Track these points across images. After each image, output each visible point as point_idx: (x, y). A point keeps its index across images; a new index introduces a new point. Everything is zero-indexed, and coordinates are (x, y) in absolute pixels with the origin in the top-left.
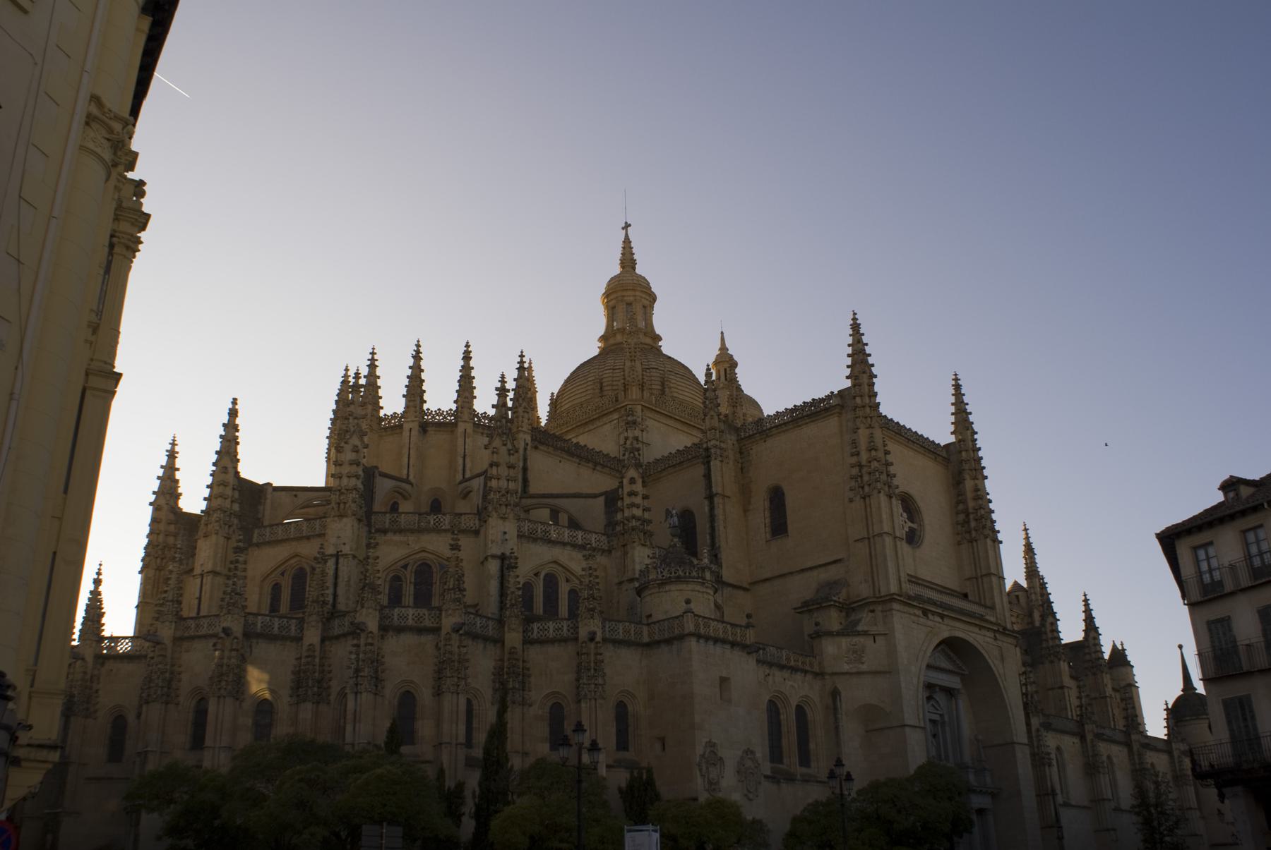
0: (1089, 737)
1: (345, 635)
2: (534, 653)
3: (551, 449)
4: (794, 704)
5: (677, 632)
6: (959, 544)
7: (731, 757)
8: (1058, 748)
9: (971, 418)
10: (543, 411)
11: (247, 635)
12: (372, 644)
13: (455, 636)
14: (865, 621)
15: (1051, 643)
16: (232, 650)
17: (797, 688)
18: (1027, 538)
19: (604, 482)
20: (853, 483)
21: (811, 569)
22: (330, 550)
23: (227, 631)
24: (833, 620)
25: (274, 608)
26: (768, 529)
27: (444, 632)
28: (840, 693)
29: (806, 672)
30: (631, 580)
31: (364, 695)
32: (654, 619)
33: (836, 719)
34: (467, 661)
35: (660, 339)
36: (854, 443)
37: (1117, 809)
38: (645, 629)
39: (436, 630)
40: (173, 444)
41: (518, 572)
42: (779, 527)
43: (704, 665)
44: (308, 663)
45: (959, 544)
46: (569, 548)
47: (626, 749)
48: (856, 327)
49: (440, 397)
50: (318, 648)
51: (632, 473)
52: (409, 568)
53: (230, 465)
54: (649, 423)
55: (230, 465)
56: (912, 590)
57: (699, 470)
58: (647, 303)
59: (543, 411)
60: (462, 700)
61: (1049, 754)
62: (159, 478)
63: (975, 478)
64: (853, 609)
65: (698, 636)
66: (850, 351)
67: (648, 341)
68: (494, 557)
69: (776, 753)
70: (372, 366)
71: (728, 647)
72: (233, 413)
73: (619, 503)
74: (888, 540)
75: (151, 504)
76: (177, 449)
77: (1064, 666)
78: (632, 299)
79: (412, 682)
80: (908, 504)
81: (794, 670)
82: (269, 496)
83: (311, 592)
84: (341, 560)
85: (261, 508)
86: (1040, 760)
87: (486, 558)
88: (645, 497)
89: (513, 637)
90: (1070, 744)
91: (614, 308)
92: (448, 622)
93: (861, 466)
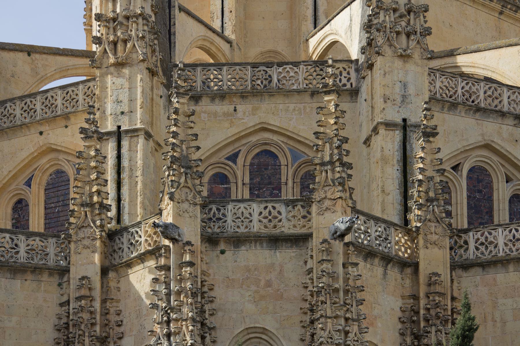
12: (191, 264)
13: (338, 246)
22: (110, 126)
27: (315, 242)
34: (361, 289)
39: (300, 240)
46: (510, 121)
79: (264, 331)
87: (375, 130)
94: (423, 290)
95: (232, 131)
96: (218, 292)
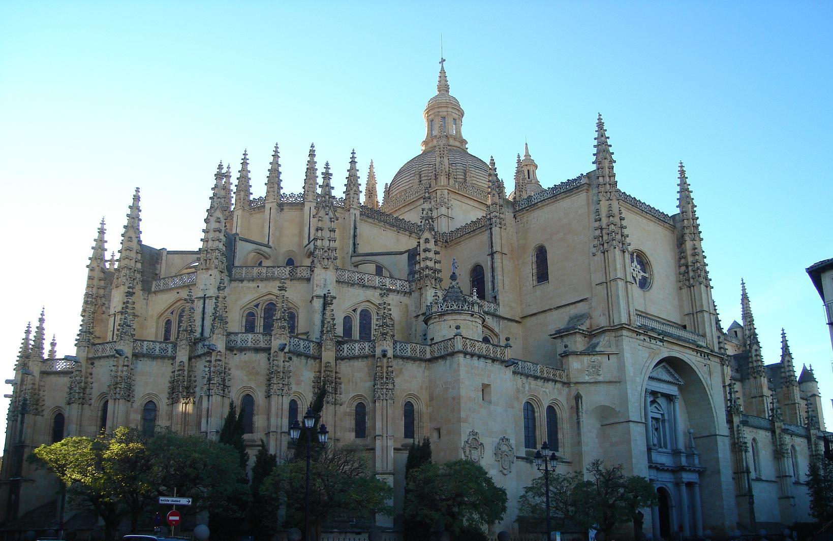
0: (778, 431)
1: (204, 354)
2: (345, 368)
4: (546, 404)
5: (450, 350)
7: (489, 443)
8: (754, 439)
9: (692, 195)
11: (136, 356)
13: (281, 354)
14: (603, 343)
15: (755, 364)
16: (124, 366)
17: (548, 394)
18: (744, 289)
19: (407, 243)
20: (596, 242)
21: (565, 306)
22: (201, 294)
23: (119, 353)
24: (578, 343)
25: (167, 338)
26: (535, 278)
27: (272, 351)
28: (581, 397)
29: (556, 381)
30: (424, 314)
31: (214, 397)
32: (435, 341)
33: (578, 418)
35: (464, 142)
36: (597, 211)
37: (797, 483)
38: (428, 348)
39: (267, 350)
40: (103, 224)
41: (332, 307)
42: (542, 275)
43: (469, 375)
44: (179, 375)
47: (413, 437)
48: (600, 125)
50: (186, 364)
51: (427, 235)
52: (260, 307)
53: (133, 236)
54: (454, 202)
55: (133, 236)
56: (638, 322)
57: (485, 237)
60: (286, 401)
61: (746, 443)
62: (93, 248)
63: (694, 240)
64: (595, 335)
65: (465, 354)
66: (595, 143)
67: (457, 144)
68: (317, 297)
69: (530, 440)
70: (245, 163)
71: (490, 361)
72: (137, 198)
73: (418, 257)
74: (621, 284)
75: (87, 266)
77: (764, 381)
78: (445, 113)
79: (251, 388)
80: (642, 260)
81: (547, 380)
82: (164, 258)
83: (184, 325)
84: (207, 301)
86: (738, 447)
88: (436, 253)
89: (328, 355)
90: (763, 437)
91: (432, 121)
92: (276, 344)
93: (602, 229)
94: (323, 369)
95: (256, 295)
96: (232, 371)
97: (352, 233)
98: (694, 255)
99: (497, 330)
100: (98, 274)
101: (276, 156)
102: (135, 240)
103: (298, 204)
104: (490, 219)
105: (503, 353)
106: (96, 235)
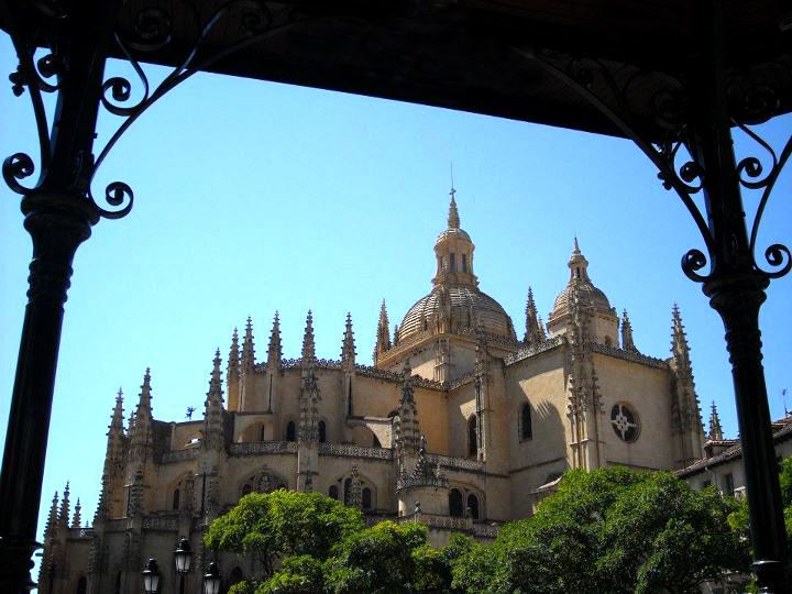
3: (373, 380)
6: (673, 435)
10: (392, 338)
11: (144, 531)
16: (134, 542)
40: (120, 393)
42: (527, 433)
45: (673, 435)
46: (361, 460)
49: (292, 351)
54: (457, 349)
58: (465, 252)
59: (392, 338)
63: (685, 384)
70: (249, 330)
72: (147, 378)
76: (123, 396)
85: (167, 439)
97: (347, 395)
98: (685, 400)
99: (482, 488)
100: (117, 441)
101: (276, 324)
102: (147, 418)
103: (296, 368)
104: (478, 378)
105: (463, 524)
106: (114, 405)
